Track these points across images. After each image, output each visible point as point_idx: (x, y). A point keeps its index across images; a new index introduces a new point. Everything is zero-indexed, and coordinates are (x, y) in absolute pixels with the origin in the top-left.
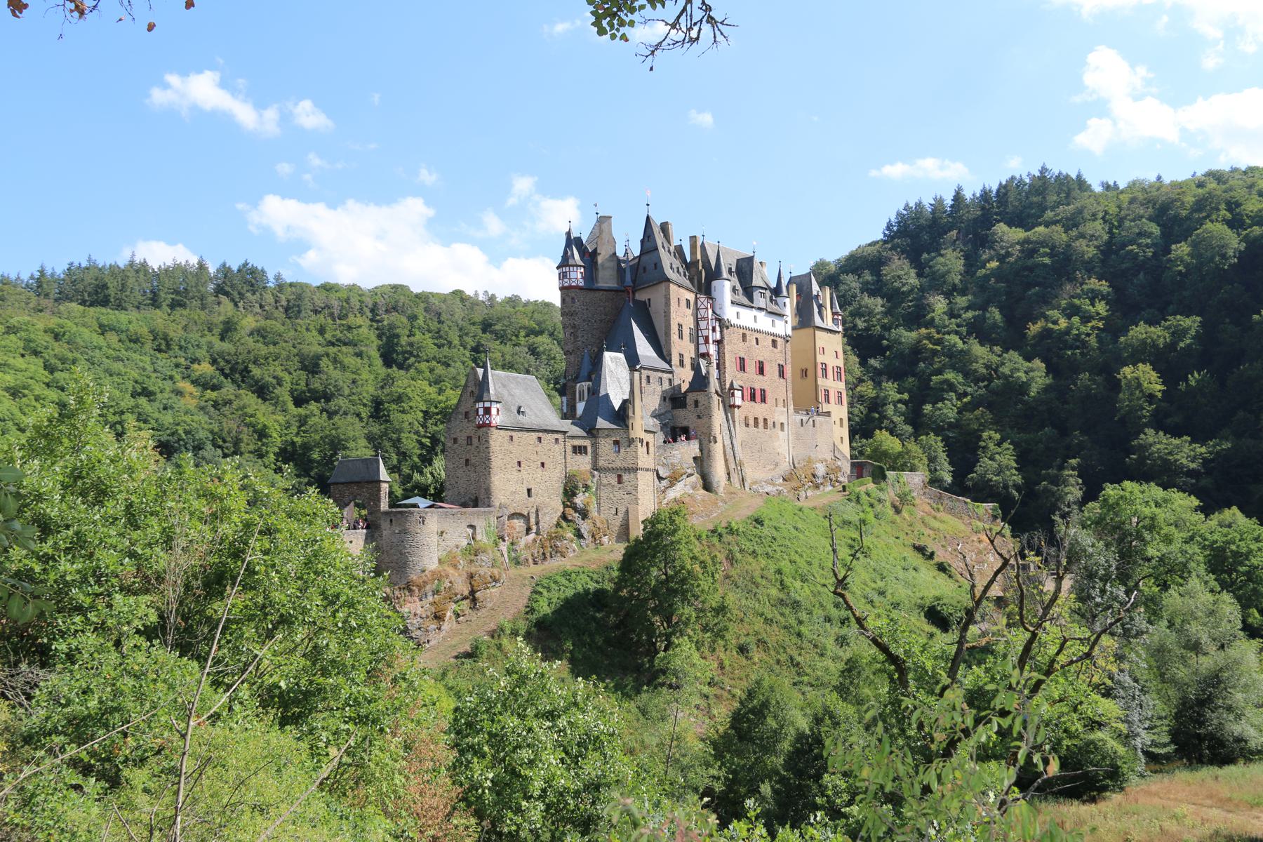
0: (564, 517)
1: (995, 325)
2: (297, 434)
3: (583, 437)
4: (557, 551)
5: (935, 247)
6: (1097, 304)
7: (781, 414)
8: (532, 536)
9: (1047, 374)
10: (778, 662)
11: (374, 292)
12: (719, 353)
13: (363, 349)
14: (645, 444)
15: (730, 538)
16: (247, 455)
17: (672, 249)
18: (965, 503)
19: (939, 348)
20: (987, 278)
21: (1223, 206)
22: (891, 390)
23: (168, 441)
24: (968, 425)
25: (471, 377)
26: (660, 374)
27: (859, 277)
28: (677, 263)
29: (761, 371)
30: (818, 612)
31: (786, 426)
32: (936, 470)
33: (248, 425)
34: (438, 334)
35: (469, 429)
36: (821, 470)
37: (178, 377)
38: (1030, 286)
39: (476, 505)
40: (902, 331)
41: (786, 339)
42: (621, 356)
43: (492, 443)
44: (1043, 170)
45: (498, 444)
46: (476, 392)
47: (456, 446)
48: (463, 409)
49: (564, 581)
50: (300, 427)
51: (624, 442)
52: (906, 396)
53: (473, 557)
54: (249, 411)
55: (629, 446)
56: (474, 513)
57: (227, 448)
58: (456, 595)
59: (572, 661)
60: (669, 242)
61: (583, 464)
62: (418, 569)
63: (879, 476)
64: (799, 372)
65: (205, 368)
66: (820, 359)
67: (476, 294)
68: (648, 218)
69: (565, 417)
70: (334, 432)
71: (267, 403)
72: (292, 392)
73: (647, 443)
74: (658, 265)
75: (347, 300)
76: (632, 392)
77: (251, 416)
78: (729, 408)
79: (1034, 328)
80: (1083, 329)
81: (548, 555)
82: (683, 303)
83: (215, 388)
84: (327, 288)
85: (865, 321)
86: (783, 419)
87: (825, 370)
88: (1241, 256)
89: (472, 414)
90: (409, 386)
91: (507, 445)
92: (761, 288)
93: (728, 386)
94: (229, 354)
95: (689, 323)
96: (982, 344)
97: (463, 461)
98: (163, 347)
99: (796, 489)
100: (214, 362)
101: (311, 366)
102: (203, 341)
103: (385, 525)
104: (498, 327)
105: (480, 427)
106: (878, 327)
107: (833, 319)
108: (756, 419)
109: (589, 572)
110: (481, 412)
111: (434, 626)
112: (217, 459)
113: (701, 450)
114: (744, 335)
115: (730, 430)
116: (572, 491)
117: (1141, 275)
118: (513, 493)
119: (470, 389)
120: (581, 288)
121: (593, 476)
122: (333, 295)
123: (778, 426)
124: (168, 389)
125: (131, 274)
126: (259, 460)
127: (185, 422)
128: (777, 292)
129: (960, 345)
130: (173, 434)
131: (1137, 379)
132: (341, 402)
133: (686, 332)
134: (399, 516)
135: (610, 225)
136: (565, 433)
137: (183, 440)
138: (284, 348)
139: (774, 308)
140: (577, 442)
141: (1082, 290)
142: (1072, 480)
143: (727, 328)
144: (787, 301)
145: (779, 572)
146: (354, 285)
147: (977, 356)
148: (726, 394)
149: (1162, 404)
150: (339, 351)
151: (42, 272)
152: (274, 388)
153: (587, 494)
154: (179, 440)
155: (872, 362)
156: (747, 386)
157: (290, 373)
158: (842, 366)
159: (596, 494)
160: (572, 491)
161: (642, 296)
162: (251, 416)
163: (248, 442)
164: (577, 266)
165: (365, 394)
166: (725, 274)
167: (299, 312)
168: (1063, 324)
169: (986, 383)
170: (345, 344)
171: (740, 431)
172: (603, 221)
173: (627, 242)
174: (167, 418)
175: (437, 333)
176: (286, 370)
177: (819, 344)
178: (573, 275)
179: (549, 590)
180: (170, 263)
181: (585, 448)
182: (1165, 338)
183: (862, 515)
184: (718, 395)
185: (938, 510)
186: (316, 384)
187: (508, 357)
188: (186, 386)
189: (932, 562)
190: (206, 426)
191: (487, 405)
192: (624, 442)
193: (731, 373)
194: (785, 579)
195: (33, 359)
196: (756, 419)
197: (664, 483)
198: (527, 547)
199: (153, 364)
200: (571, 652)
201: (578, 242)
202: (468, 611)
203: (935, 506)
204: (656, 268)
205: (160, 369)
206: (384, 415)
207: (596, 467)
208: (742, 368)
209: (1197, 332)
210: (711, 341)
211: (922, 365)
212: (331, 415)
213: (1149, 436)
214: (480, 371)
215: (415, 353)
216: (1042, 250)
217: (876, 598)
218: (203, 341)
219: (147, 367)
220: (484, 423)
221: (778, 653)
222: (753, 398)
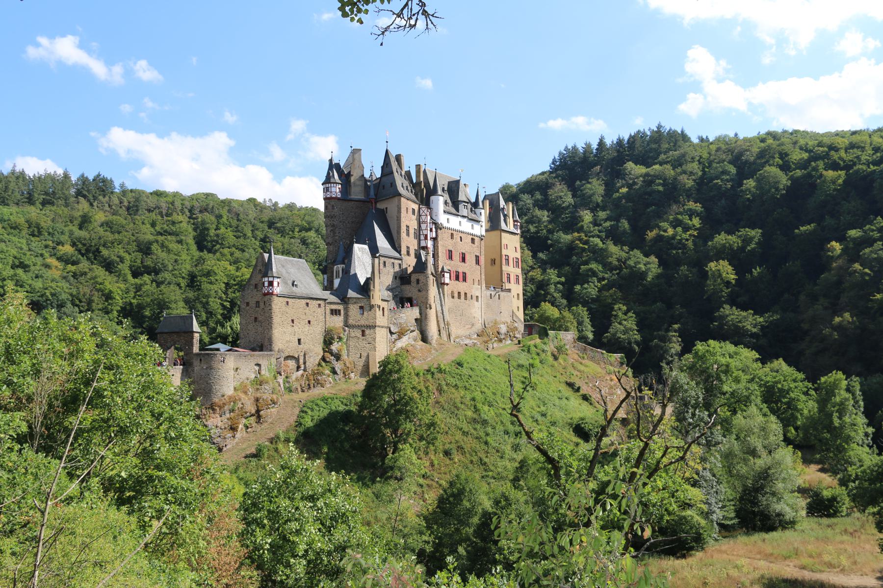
0: (323, 359)
1: (624, 231)
2: (134, 298)
3: (338, 303)
4: (318, 383)
5: (585, 177)
6: (693, 219)
7: (476, 290)
8: (301, 372)
9: (659, 266)
10: (472, 462)
11: (192, 198)
12: (434, 247)
13: (183, 238)
14: (381, 308)
15: (439, 375)
16: (97, 312)
17: (403, 173)
18: (602, 353)
19: (586, 247)
20: (620, 198)
21: (777, 155)
22: (553, 275)
23: (38, 301)
24: (605, 300)
25: (260, 260)
26: (393, 260)
27: (532, 196)
28: (406, 183)
29: (463, 260)
30: (500, 428)
32: (582, 330)
33: (98, 290)
34: (237, 229)
35: (258, 296)
36: (503, 329)
37: (47, 255)
38: (648, 205)
39: (261, 350)
40: (561, 234)
41: (481, 238)
42: (366, 247)
43: (273, 306)
44: (659, 127)
46: (263, 270)
47: (248, 308)
48: (253, 282)
49: (322, 404)
50: (136, 292)
51: (367, 307)
52: (563, 279)
53: (258, 387)
54: (100, 280)
55: (370, 310)
56: (260, 356)
57: (82, 306)
58: (246, 413)
59: (327, 460)
60: (401, 168)
61: (337, 322)
62: (219, 394)
63: (543, 334)
64: (489, 261)
65: (67, 249)
66: (504, 252)
67: (265, 201)
68: (387, 151)
69: (325, 289)
70: (161, 296)
71: (113, 274)
72: (131, 267)
73: (383, 308)
74: (393, 184)
75: (173, 203)
76: (373, 272)
77: (101, 284)
78: (441, 285)
79: (651, 235)
80: (684, 236)
81: (312, 386)
82: (410, 211)
83: (74, 263)
84: (158, 194)
85: (536, 227)
86: (478, 293)
87: (507, 260)
88: (788, 189)
89: (260, 285)
90: (216, 265)
91: (284, 308)
92: (465, 202)
93: (440, 270)
94: (85, 239)
95: (414, 225)
96: (615, 244)
97: (253, 318)
98: (36, 233)
99: (486, 342)
100: (74, 244)
101: (145, 249)
102: (66, 229)
103: (196, 363)
104: (279, 225)
105: (265, 294)
106: (545, 231)
107: (514, 225)
108: (459, 293)
109: (340, 398)
110: (266, 284)
111: (230, 435)
112: (75, 314)
113: (421, 314)
114: (452, 235)
115: (441, 300)
116: (329, 341)
117: (723, 201)
118: (288, 342)
119: (258, 268)
120: (338, 199)
121: (345, 331)
122: (163, 199)
123: (474, 298)
124: (39, 263)
125: (13, 179)
126: (106, 316)
127: (52, 287)
128: (475, 205)
129: (601, 245)
130: (42, 296)
131: (719, 270)
132: (167, 275)
133: (412, 231)
134: (206, 357)
135: (360, 155)
136: (325, 300)
137: (50, 300)
138: (126, 236)
139: (473, 216)
140: (334, 307)
141: (684, 209)
142: (674, 339)
143: (441, 229)
144: (483, 211)
145: (473, 399)
146: (177, 192)
147: (612, 253)
148: (439, 275)
149: (736, 288)
150: (165, 239)
152: (118, 264)
153: (340, 343)
154: (47, 300)
155: (541, 255)
156: (453, 270)
157: (130, 254)
158: (519, 258)
159: (346, 344)
160: (329, 341)
161: (380, 206)
162: (101, 284)
163: (98, 302)
164: (336, 183)
165: (183, 270)
166: (440, 192)
167: (137, 210)
168: (671, 232)
169: (618, 271)
170: (170, 234)
171: (448, 301)
172: (355, 152)
173: (372, 168)
174: (38, 284)
175: (237, 228)
176: (127, 251)
177: (504, 242)
178: (333, 189)
179: (312, 410)
180: (42, 172)
181: (339, 311)
182: (738, 243)
183: (531, 361)
184: (433, 276)
185: (583, 358)
186: (149, 262)
187: (286, 246)
188: (53, 261)
189: (578, 394)
190: (67, 291)
191: (271, 279)
192: (367, 308)
193: (443, 261)
194: (478, 404)
196: (459, 293)
197: (394, 336)
198: (297, 379)
199: (28, 245)
200: (326, 453)
201: (338, 166)
202: (254, 425)
203: (581, 355)
204: (391, 186)
205: (34, 249)
206: (197, 285)
207: (346, 324)
208: (450, 257)
209: (759, 239)
210: (429, 238)
211: (574, 258)
212: (159, 284)
213: (727, 309)
214: (266, 256)
215: (220, 241)
216: (657, 181)
217: (540, 418)
218: (66, 229)
219: (23, 247)
220: (268, 292)
221: (471, 455)
222: (457, 278)
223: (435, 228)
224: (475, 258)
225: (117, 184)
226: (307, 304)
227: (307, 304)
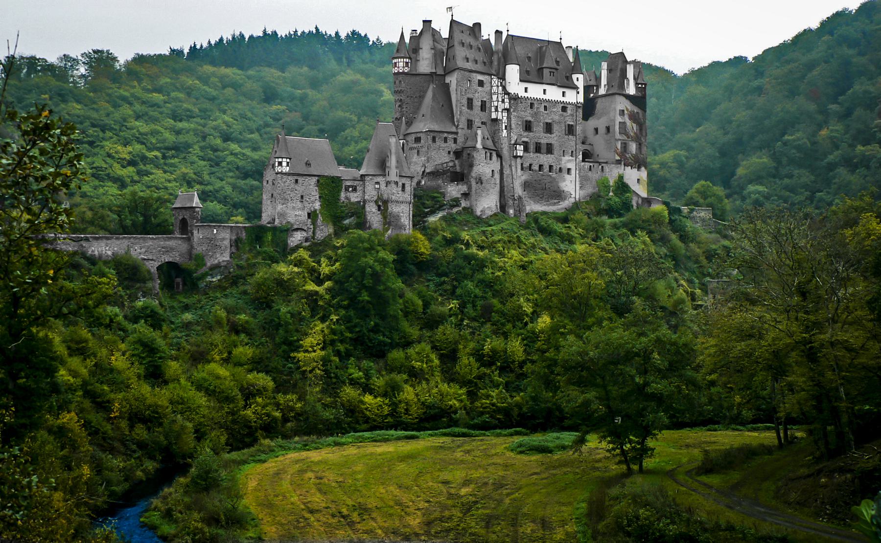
7: (568, 162)
26: (446, 135)
29: (548, 128)
31: (573, 172)
41: (576, 106)
45: (286, 184)
55: (386, 186)
73: (404, 185)
86: (571, 165)
91: (292, 186)
93: (513, 142)
97: (270, 195)
133: (477, 104)
140: (348, 183)
191: (280, 160)
210: (500, 110)
222: (538, 149)
223: (510, 99)
225: (372, 38)
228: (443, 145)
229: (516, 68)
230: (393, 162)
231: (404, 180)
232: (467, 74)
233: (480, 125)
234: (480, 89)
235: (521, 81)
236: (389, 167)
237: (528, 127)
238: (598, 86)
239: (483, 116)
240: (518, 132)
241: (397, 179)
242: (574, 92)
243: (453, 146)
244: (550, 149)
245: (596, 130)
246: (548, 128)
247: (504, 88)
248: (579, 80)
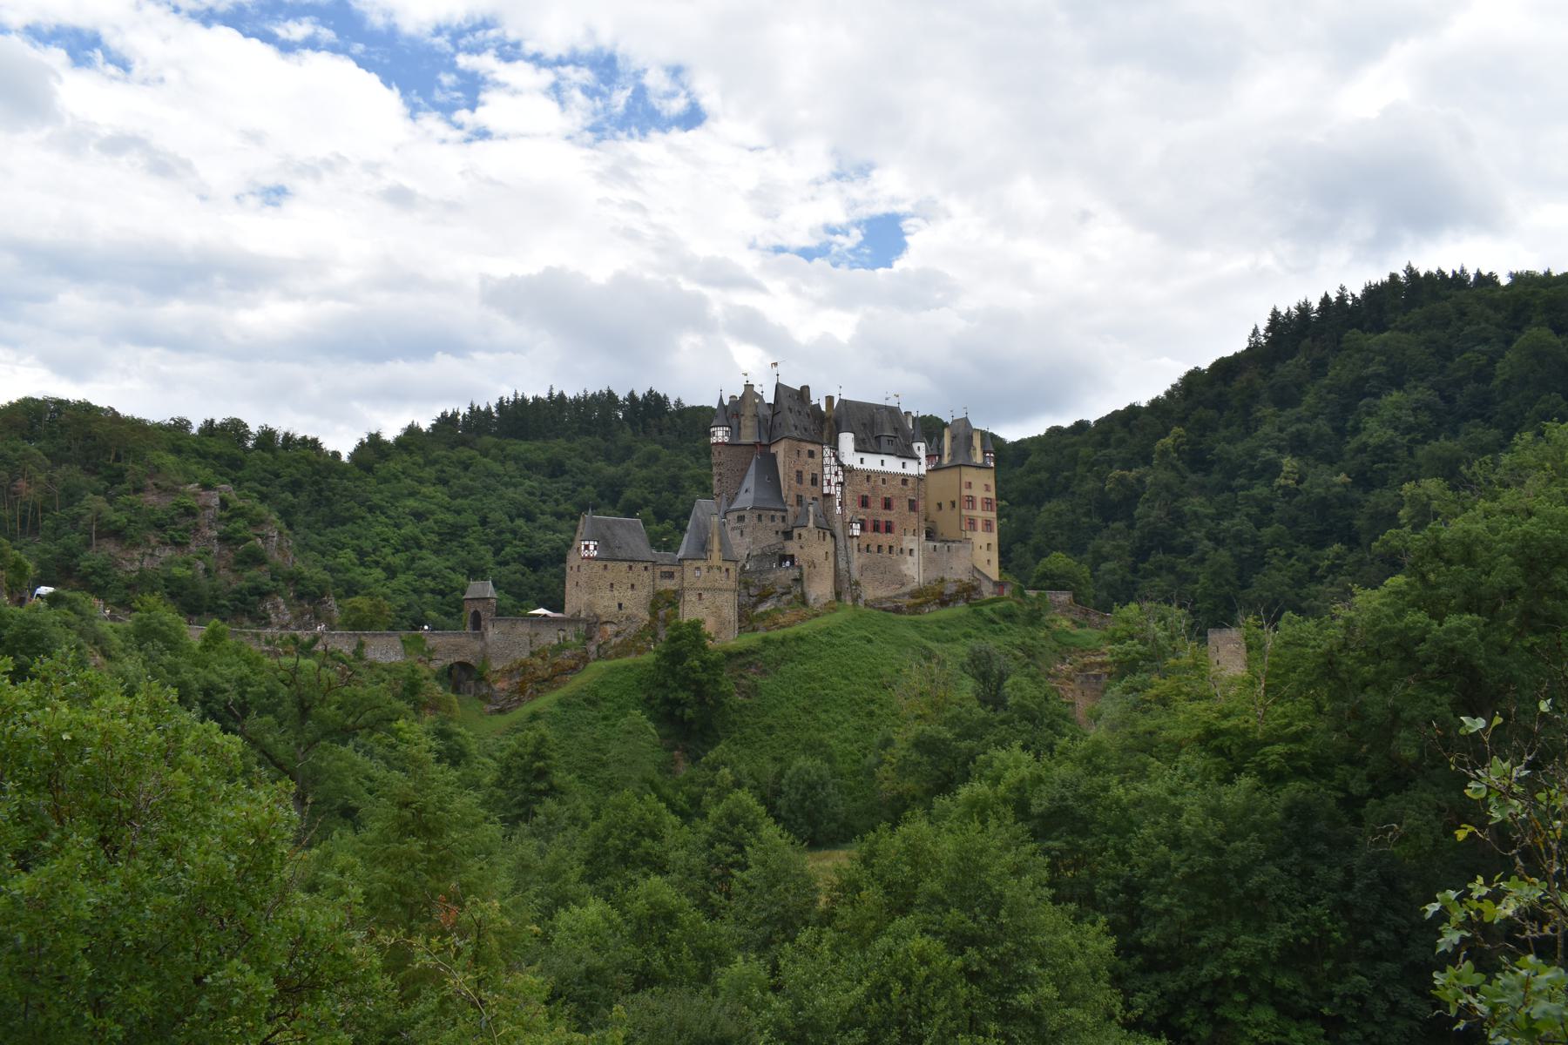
7: (910, 542)
26: (773, 513)
29: (887, 505)
41: (920, 479)
73: (727, 570)
86: (914, 546)
107: (985, 457)
108: (879, 547)
133: (807, 477)
140: (665, 569)
151: (471, 408)
177: (966, 479)
195: (440, 487)
222: (876, 528)
224: (906, 504)
225: (672, 402)
226: (630, 567)
227: (630, 567)
228: (770, 524)
229: (850, 436)
230: (716, 545)
231: (728, 565)
232: (795, 443)
233: (811, 501)
234: (810, 460)
235: (856, 451)
236: (711, 551)
237: (864, 502)
238: (941, 456)
239: (815, 491)
240: (853, 508)
241: (720, 563)
242: (915, 463)
243: (781, 525)
244: (889, 528)
245: (940, 505)
246: (887, 505)
247: (837, 459)
248: (920, 448)
